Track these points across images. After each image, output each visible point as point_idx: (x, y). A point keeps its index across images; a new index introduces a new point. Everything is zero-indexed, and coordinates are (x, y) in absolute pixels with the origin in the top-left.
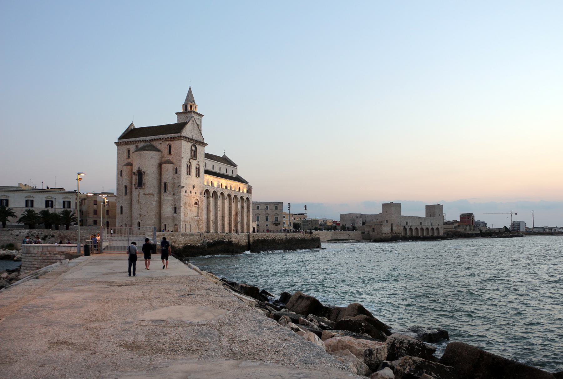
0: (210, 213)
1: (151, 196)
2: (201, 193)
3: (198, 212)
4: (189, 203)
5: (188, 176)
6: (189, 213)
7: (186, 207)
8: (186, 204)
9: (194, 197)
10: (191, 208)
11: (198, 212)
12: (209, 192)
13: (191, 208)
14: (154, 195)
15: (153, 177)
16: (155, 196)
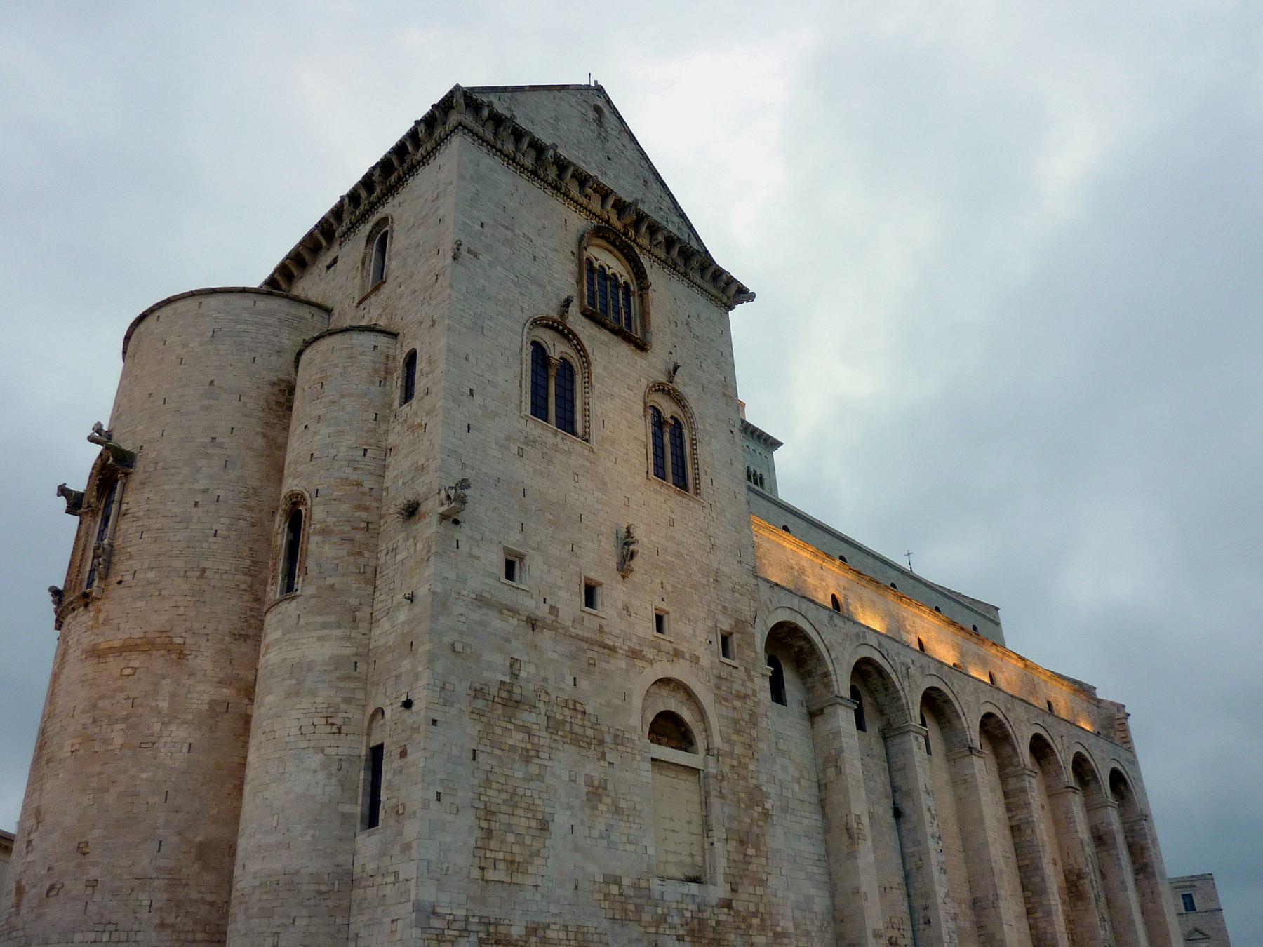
0: (852, 855)
1: (158, 662)
2: (725, 640)
3: (707, 829)
4: (575, 706)
5: (546, 432)
6: (562, 820)
7: (516, 738)
8: (512, 703)
9: (635, 654)
10: (594, 769)
11: (707, 829)
12: (820, 659)
13: (594, 769)
14: (182, 654)
15: (203, 484)
16: (204, 660)
